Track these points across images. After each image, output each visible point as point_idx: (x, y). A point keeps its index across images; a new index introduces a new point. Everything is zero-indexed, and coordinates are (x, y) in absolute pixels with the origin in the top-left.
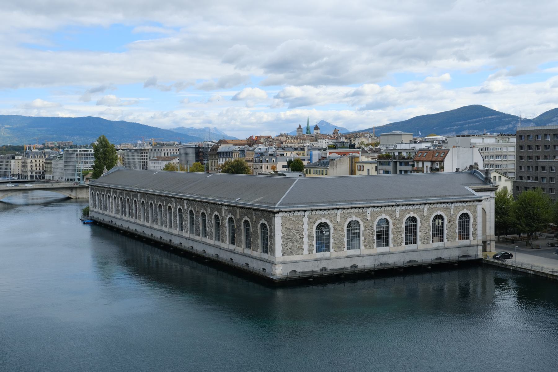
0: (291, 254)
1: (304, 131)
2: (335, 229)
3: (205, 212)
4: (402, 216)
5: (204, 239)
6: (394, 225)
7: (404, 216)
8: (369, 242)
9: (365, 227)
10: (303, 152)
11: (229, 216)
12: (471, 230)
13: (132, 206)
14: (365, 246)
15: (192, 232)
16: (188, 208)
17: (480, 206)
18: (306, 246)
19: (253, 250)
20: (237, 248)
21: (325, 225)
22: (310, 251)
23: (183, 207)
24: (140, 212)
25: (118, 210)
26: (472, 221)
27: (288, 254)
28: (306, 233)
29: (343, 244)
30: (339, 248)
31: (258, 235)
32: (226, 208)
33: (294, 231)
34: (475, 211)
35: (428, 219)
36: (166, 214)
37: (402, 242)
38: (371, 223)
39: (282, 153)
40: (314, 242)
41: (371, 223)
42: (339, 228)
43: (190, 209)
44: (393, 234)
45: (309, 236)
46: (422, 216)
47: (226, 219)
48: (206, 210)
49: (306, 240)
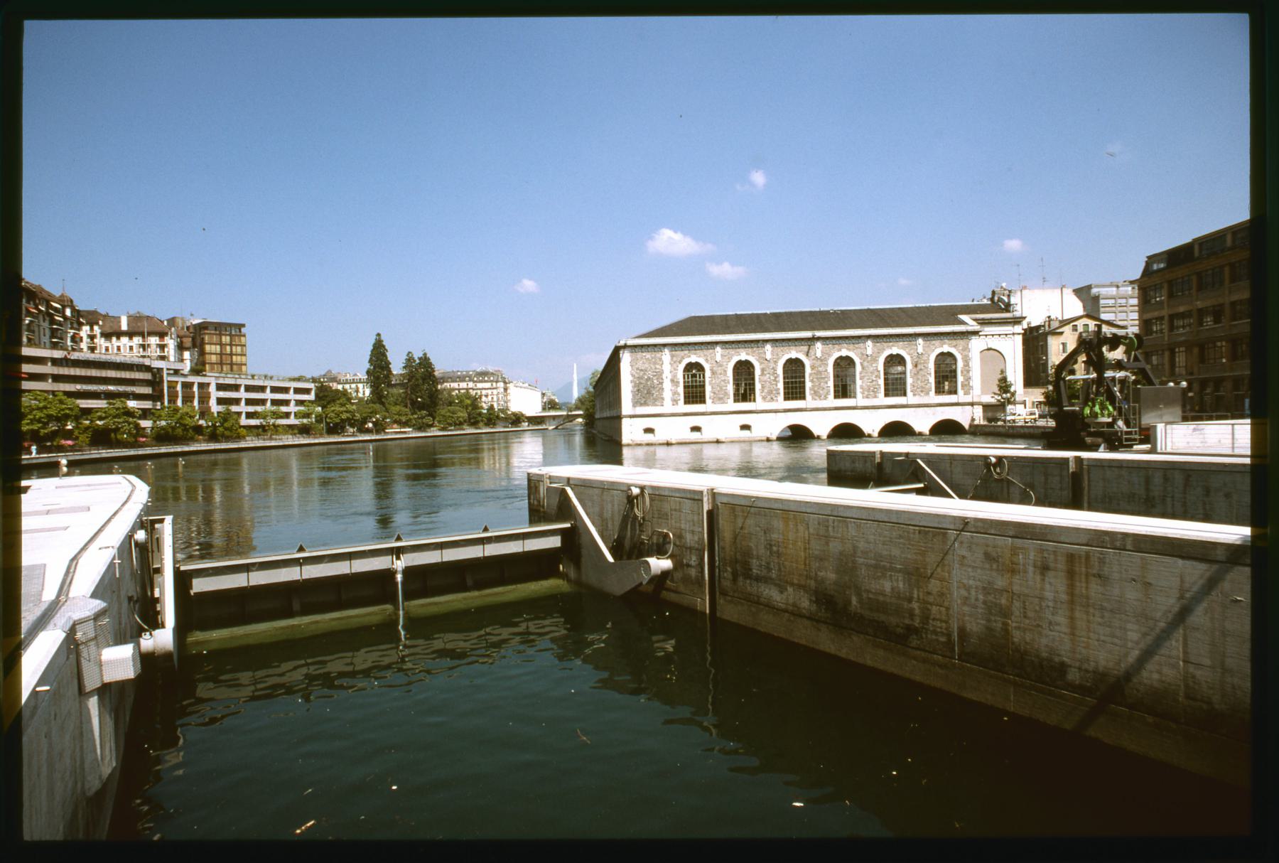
0: (645, 404)
2: (713, 373)
4: (826, 355)
6: (813, 367)
7: (830, 356)
8: (770, 392)
9: (763, 370)
12: (960, 379)
14: (764, 398)
17: (976, 344)
18: (667, 394)
21: (699, 367)
22: (675, 402)
26: (960, 364)
27: (641, 405)
28: (667, 375)
29: (726, 394)
30: (720, 399)
33: (650, 374)
34: (966, 349)
35: (875, 360)
37: (828, 393)
38: (772, 365)
40: (681, 390)
41: (772, 365)
42: (719, 370)
44: (812, 381)
45: (672, 381)
46: (864, 356)
49: (667, 385)
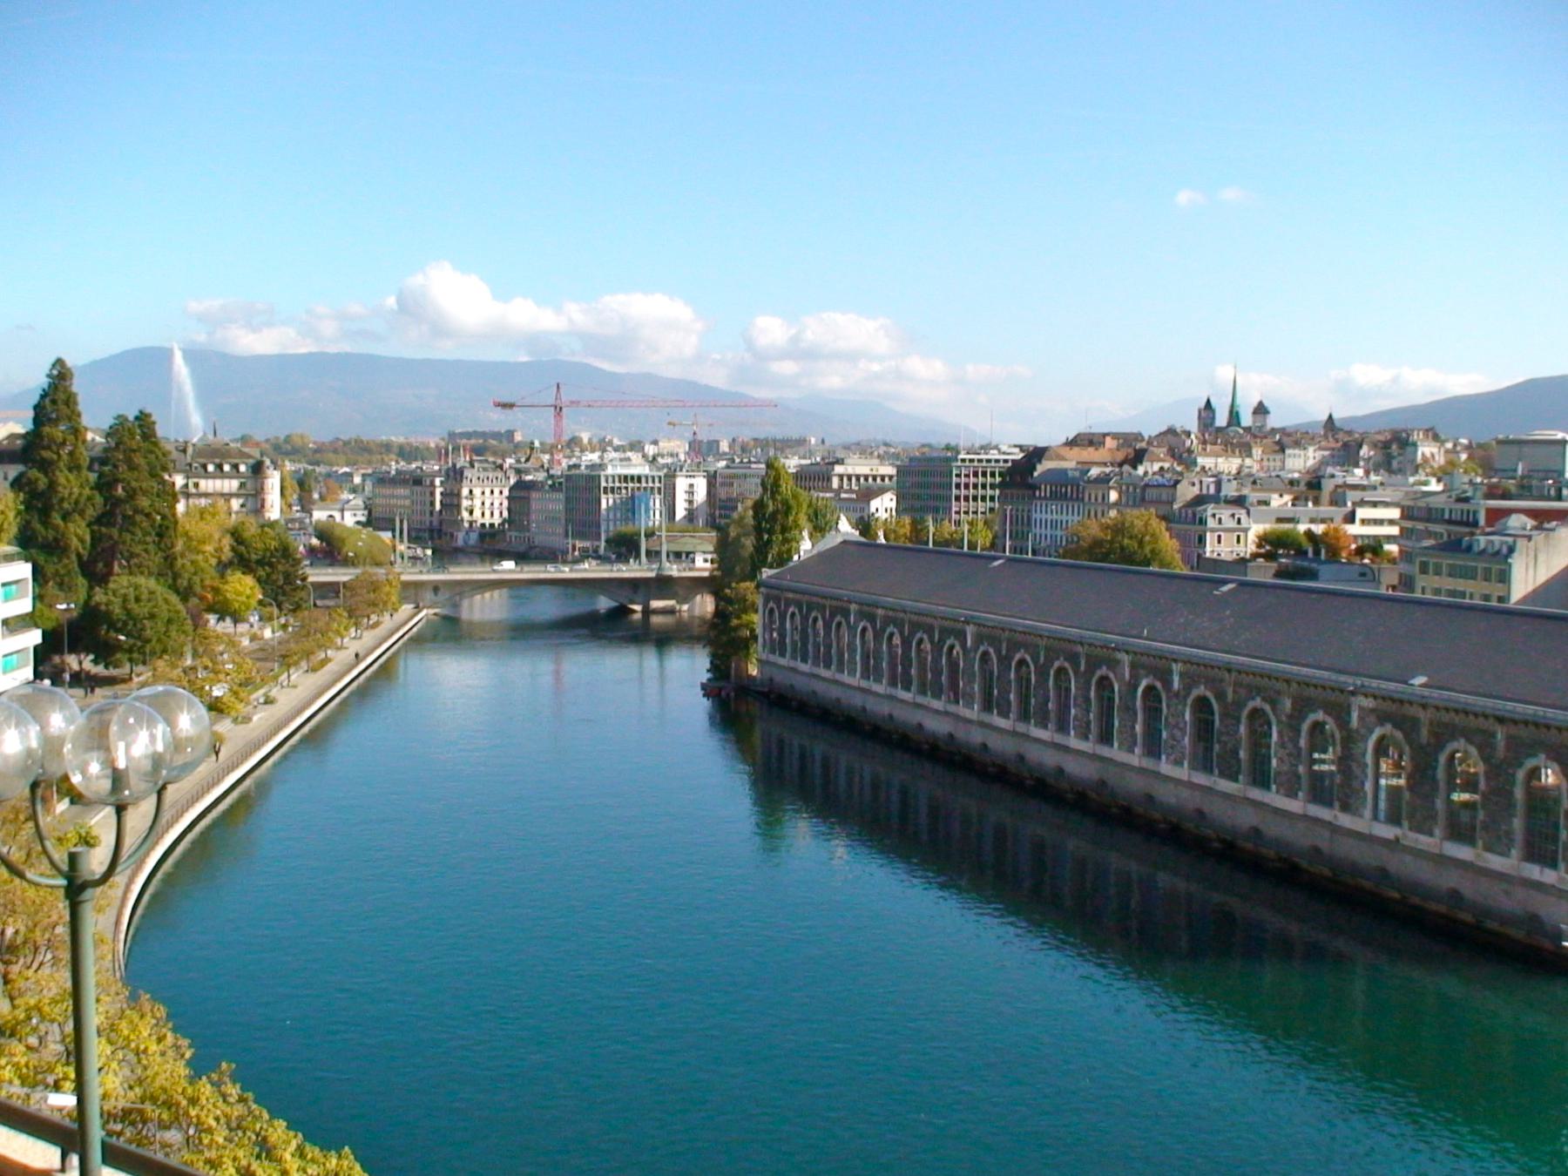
1: (1221, 420)
3: (1267, 708)
5: (1256, 794)
10: (1315, 493)
11: (1378, 732)
13: (937, 660)
15: (1206, 765)
16: (1188, 688)
19: (1488, 849)
20: (1412, 835)
23: (1167, 684)
24: (971, 682)
25: (878, 668)
31: (1511, 805)
32: (1368, 703)
36: (1087, 700)
39: (1262, 496)
43: (1195, 693)
47: (1365, 739)
48: (1274, 703)
